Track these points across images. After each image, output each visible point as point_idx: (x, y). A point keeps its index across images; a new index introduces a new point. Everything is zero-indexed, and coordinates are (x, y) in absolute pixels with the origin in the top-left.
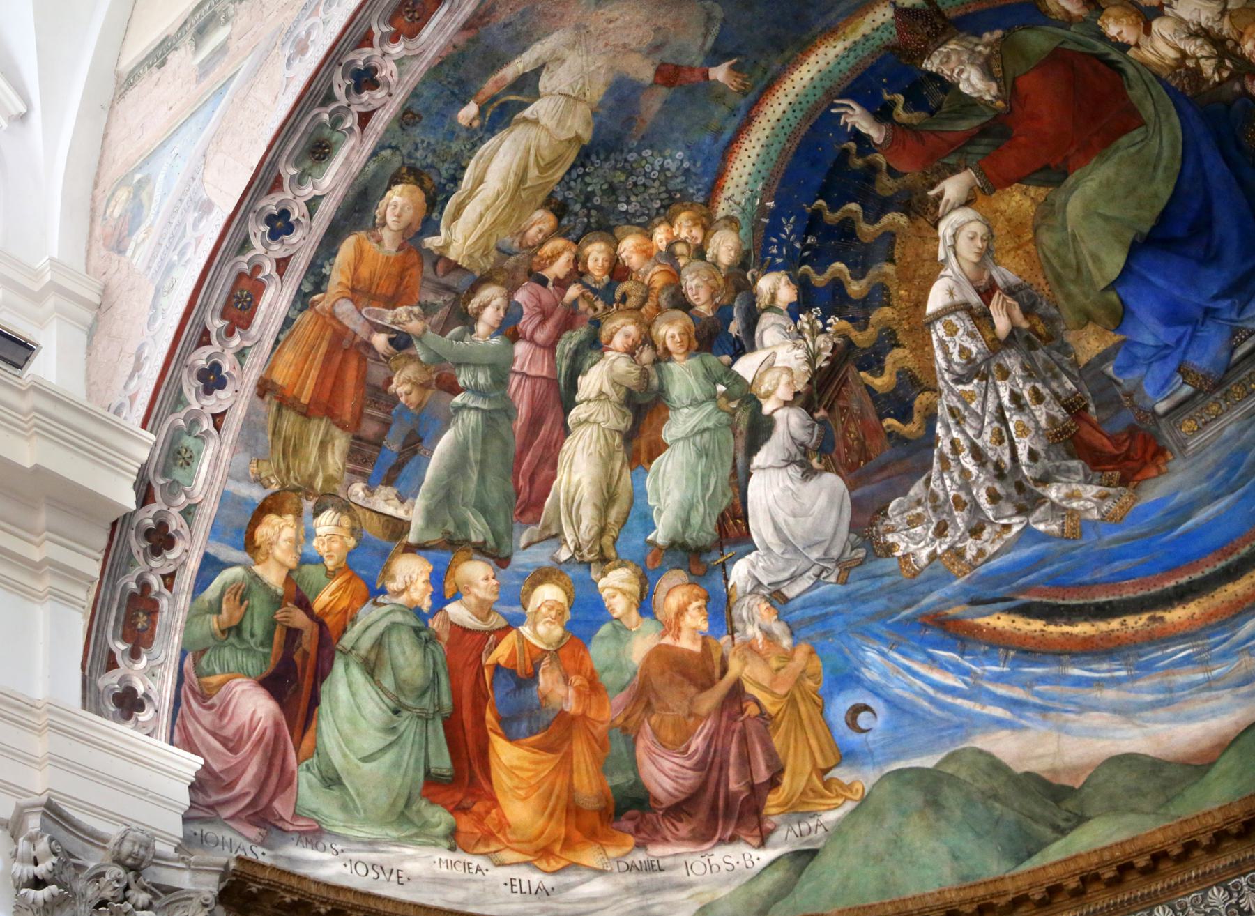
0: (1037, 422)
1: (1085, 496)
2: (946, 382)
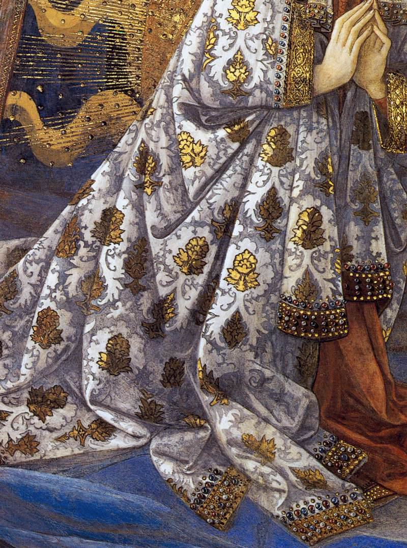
0: (280, 277)
1: (279, 461)
2: (169, 100)
